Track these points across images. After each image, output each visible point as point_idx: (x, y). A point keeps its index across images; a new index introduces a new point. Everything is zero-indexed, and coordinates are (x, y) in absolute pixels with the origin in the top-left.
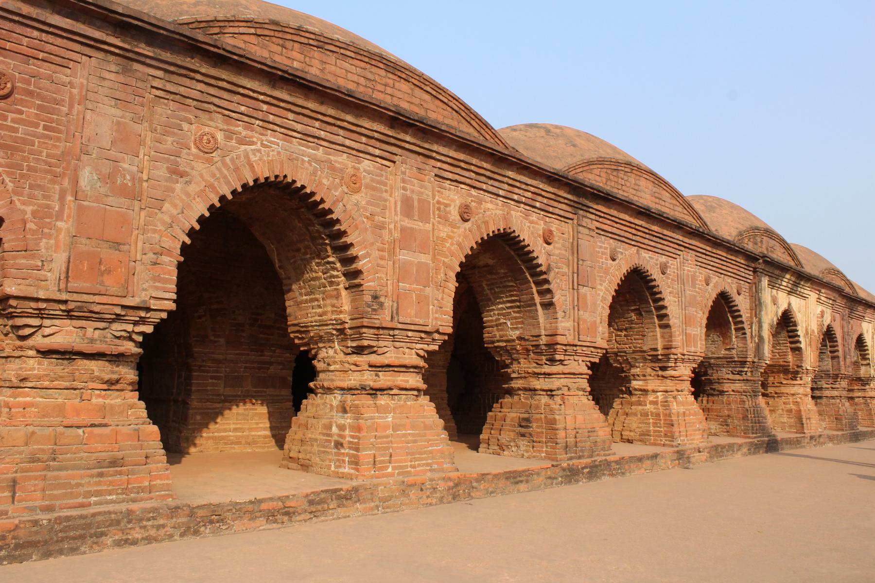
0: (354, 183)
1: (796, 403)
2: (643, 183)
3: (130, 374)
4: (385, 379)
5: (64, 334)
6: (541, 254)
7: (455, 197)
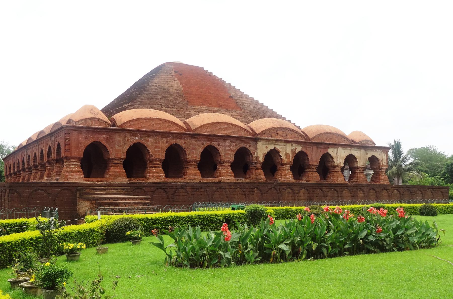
0: (148, 141)
1: (282, 172)
2: (222, 125)
3: (122, 165)
4: (154, 166)
5: (116, 162)
6: (183, 146)
7: (165, 140)
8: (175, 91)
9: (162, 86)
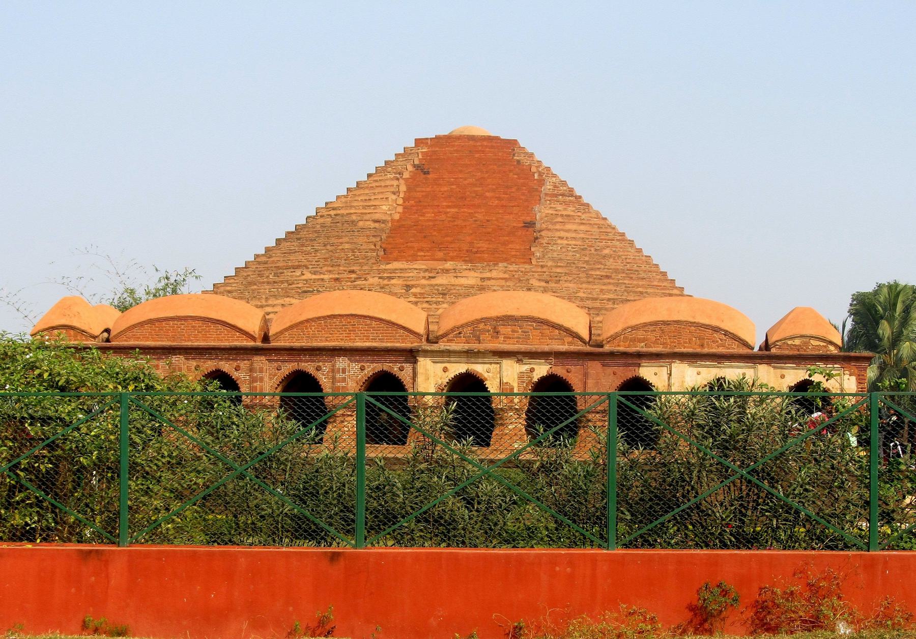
7: (194, 363)
8: (373, 225)
9: (343, 215)
